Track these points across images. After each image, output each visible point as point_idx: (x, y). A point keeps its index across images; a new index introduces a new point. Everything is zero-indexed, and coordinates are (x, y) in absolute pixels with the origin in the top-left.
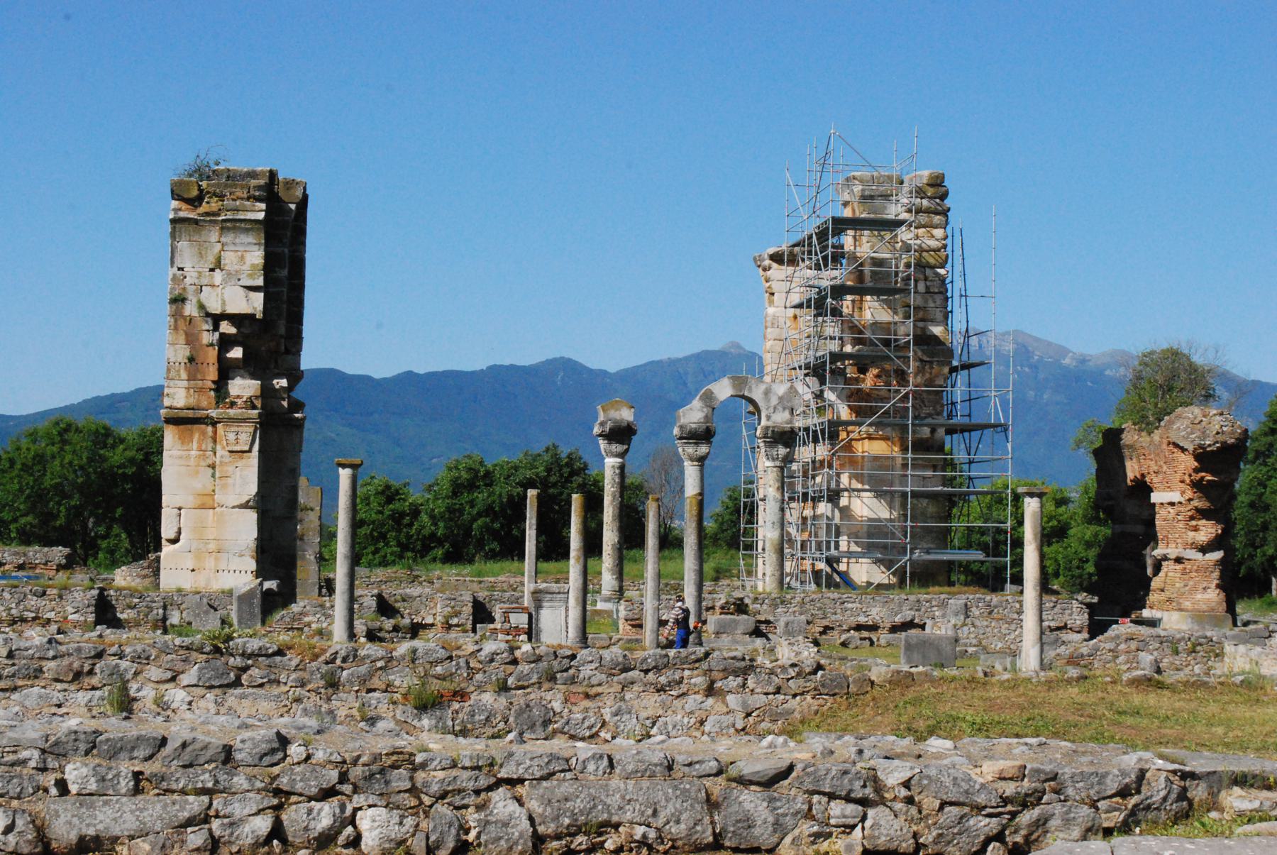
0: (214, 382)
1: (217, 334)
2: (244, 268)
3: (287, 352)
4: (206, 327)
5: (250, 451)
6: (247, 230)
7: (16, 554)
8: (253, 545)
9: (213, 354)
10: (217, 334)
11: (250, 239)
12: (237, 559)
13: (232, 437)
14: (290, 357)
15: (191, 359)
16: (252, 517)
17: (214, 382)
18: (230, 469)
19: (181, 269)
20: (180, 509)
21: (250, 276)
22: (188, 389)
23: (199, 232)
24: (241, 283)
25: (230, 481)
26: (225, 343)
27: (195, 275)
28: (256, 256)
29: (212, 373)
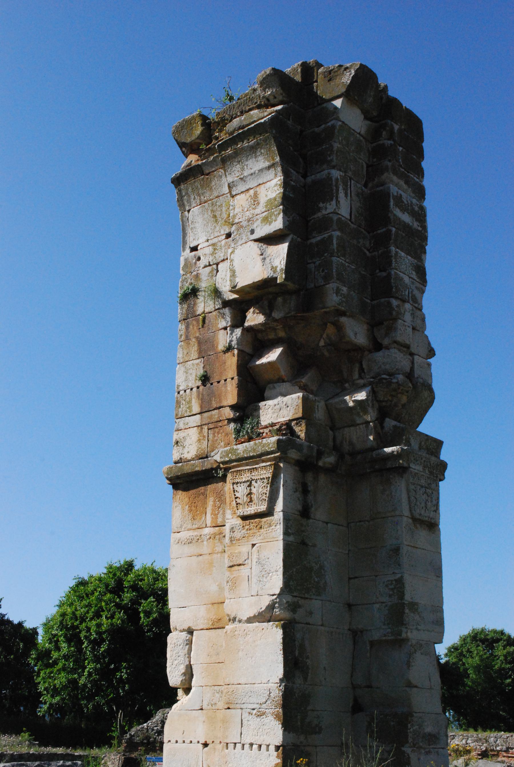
0: (233, 407)
1: (238, 332)
2: (258, 211)
3: (378, 347)
4: (223, 324)
5: (269, 513)
6: (253, 150)
7: (478, 740)
8: (277, 693)
9: (232, 361)
10: (238, 332)
11: (258, 163)
12: (252, 722)
13: (242, 490)
14: (379, 356)
15: (205, 379)
16: (273, 635)
17: (233, 407)
18: (244, 548)
19: (194, 249)
20: (191, 632)
21: (266, 220)
22: (200, 426)
23: (207, 185)
24: (256, 236)
25: (244, 571)
26: (256, 342)
27: (210, 249)
28: (272, 186)
29: (230, 394)
